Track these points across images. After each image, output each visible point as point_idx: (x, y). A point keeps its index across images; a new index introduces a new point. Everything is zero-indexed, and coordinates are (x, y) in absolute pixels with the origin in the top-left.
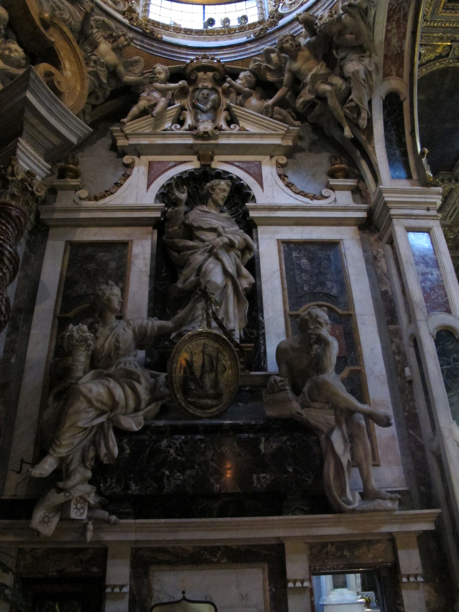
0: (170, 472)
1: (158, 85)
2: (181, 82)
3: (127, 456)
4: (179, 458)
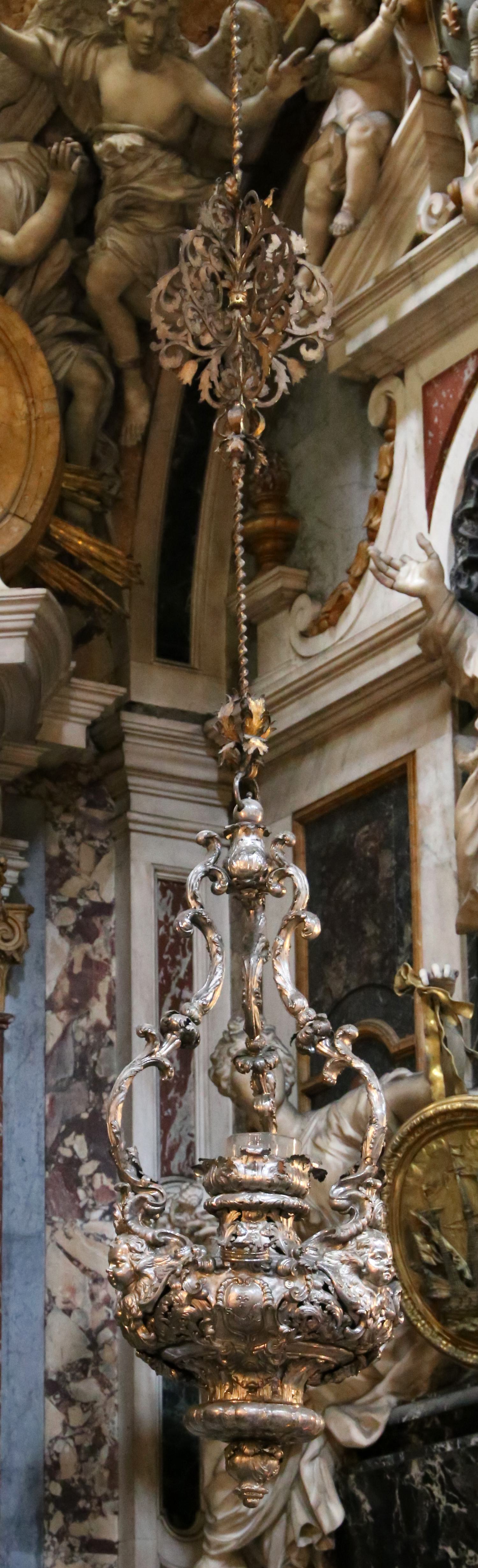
0: (455, 1549)
1: (342, 56)
2: (383, 9)
3: (371, 1519)
4: (455, 1508)
